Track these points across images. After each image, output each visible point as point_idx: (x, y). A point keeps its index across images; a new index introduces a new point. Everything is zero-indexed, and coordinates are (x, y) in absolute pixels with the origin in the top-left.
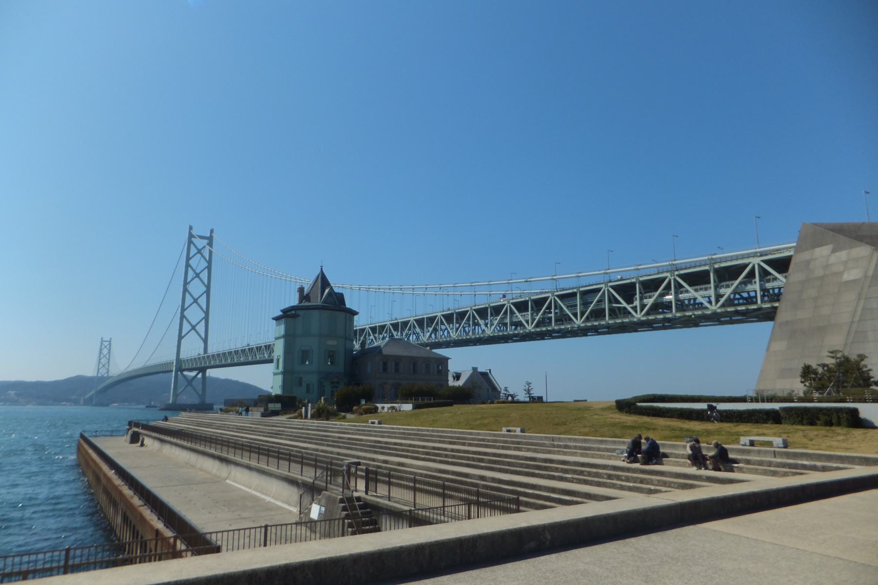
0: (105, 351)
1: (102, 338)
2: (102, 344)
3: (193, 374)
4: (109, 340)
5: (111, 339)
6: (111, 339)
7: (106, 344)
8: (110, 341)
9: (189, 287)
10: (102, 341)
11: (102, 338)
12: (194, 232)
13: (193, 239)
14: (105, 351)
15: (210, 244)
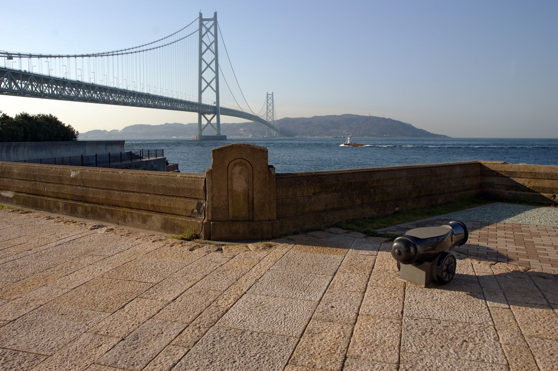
0: (270, 101)
1: (267, 93)
2: (267, 96)
3: (212, 116)
4: (272, 94)
5: (273, 93)
6: (273, 93)
7: (270, 96)
8: (273, 95)
9: (213, 56)
10: (268, 95)
11: (267, 93)
12: (204, 17)
13: (205, 23)
14: (270, 101)
15: (216, 24)
